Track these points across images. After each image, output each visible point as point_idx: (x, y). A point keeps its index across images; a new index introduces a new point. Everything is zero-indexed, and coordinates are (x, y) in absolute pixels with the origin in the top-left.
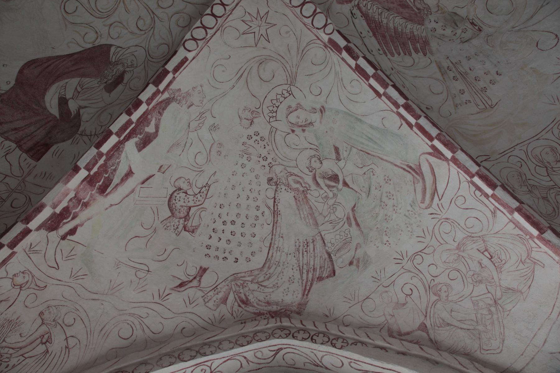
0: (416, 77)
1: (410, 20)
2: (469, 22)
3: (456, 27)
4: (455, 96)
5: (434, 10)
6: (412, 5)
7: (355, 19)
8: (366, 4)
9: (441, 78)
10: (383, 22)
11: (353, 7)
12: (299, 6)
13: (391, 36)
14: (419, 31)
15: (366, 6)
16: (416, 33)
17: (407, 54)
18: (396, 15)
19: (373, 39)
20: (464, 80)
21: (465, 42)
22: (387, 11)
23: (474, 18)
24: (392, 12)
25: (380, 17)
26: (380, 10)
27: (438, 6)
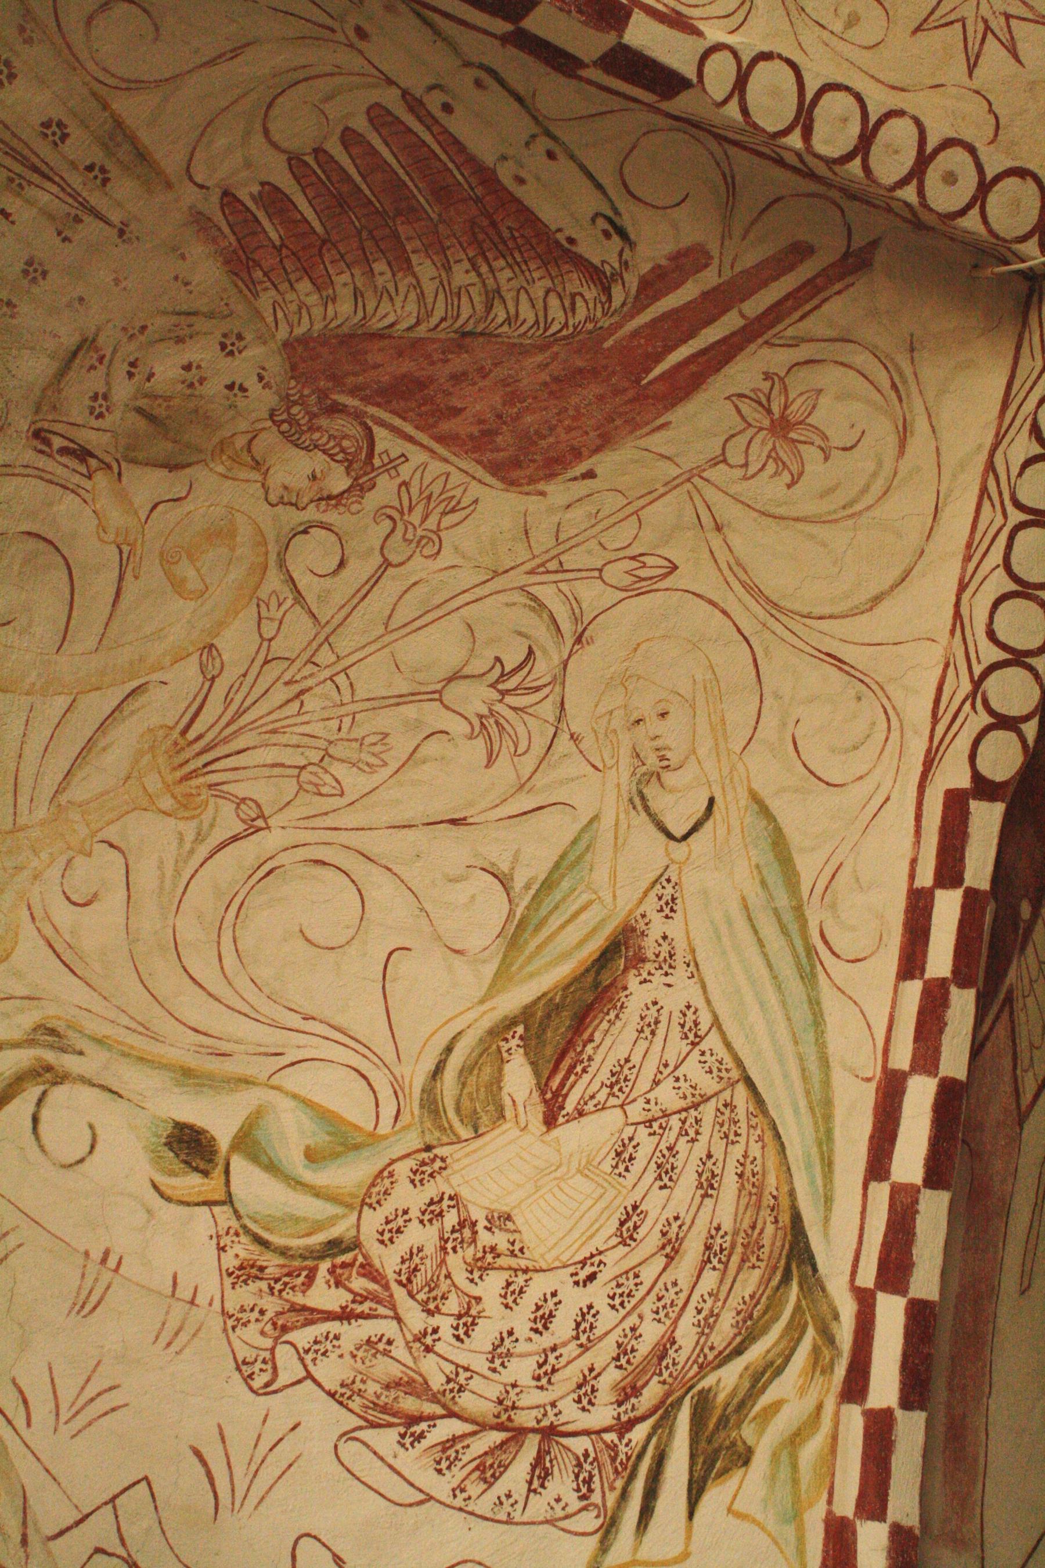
0: (235, 53)
1: (351, 336)
2: (98, 452)
3: (142, 403)
4: (22, 29)
5: (269, 439)
6: (372, 410)
7: (597, 215)
8: (573, 310)
9: (125, 106)
10: (466, 265)
11: (626, 263)
12: (880, 123)
13: (411, 212)
14: (293, 307)
15: (567, 304)
16: (305, 286)
17: (310, 160)
18: (422, 331)
19: (484, 149)
20: (14, 143)
21: (79, 349)
22: (469, 328)
23: (88, 484)
24: (442, 336)
25: (490, 282)
26: (502, 316)
27: (257, 465)
